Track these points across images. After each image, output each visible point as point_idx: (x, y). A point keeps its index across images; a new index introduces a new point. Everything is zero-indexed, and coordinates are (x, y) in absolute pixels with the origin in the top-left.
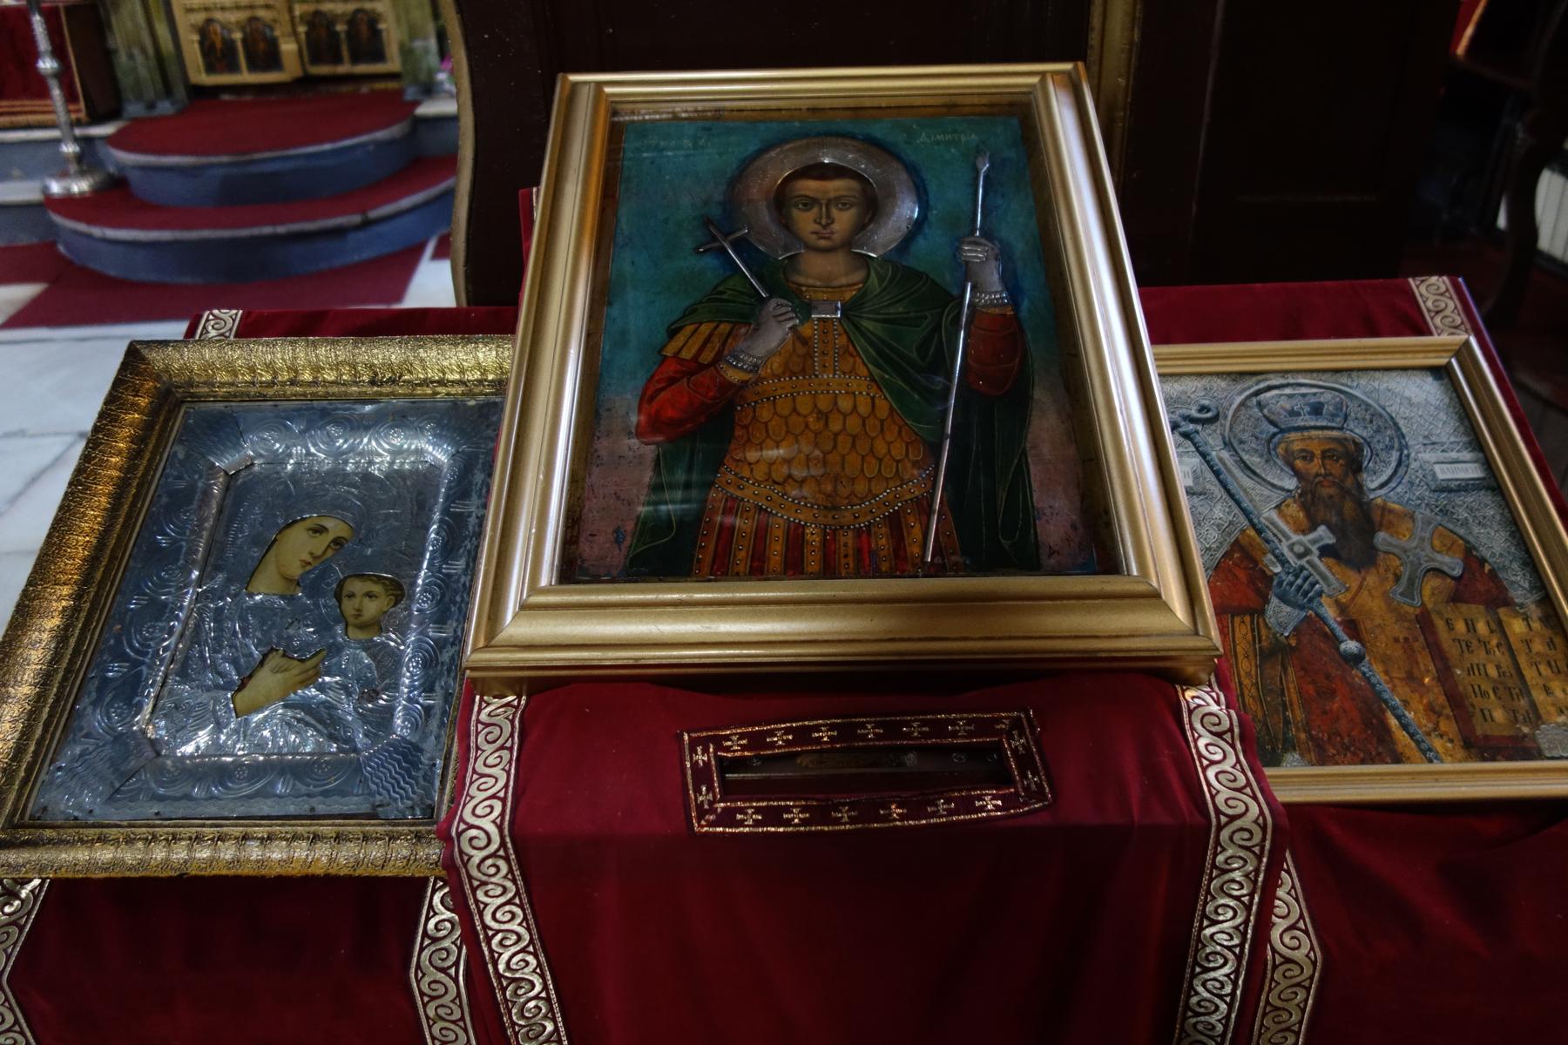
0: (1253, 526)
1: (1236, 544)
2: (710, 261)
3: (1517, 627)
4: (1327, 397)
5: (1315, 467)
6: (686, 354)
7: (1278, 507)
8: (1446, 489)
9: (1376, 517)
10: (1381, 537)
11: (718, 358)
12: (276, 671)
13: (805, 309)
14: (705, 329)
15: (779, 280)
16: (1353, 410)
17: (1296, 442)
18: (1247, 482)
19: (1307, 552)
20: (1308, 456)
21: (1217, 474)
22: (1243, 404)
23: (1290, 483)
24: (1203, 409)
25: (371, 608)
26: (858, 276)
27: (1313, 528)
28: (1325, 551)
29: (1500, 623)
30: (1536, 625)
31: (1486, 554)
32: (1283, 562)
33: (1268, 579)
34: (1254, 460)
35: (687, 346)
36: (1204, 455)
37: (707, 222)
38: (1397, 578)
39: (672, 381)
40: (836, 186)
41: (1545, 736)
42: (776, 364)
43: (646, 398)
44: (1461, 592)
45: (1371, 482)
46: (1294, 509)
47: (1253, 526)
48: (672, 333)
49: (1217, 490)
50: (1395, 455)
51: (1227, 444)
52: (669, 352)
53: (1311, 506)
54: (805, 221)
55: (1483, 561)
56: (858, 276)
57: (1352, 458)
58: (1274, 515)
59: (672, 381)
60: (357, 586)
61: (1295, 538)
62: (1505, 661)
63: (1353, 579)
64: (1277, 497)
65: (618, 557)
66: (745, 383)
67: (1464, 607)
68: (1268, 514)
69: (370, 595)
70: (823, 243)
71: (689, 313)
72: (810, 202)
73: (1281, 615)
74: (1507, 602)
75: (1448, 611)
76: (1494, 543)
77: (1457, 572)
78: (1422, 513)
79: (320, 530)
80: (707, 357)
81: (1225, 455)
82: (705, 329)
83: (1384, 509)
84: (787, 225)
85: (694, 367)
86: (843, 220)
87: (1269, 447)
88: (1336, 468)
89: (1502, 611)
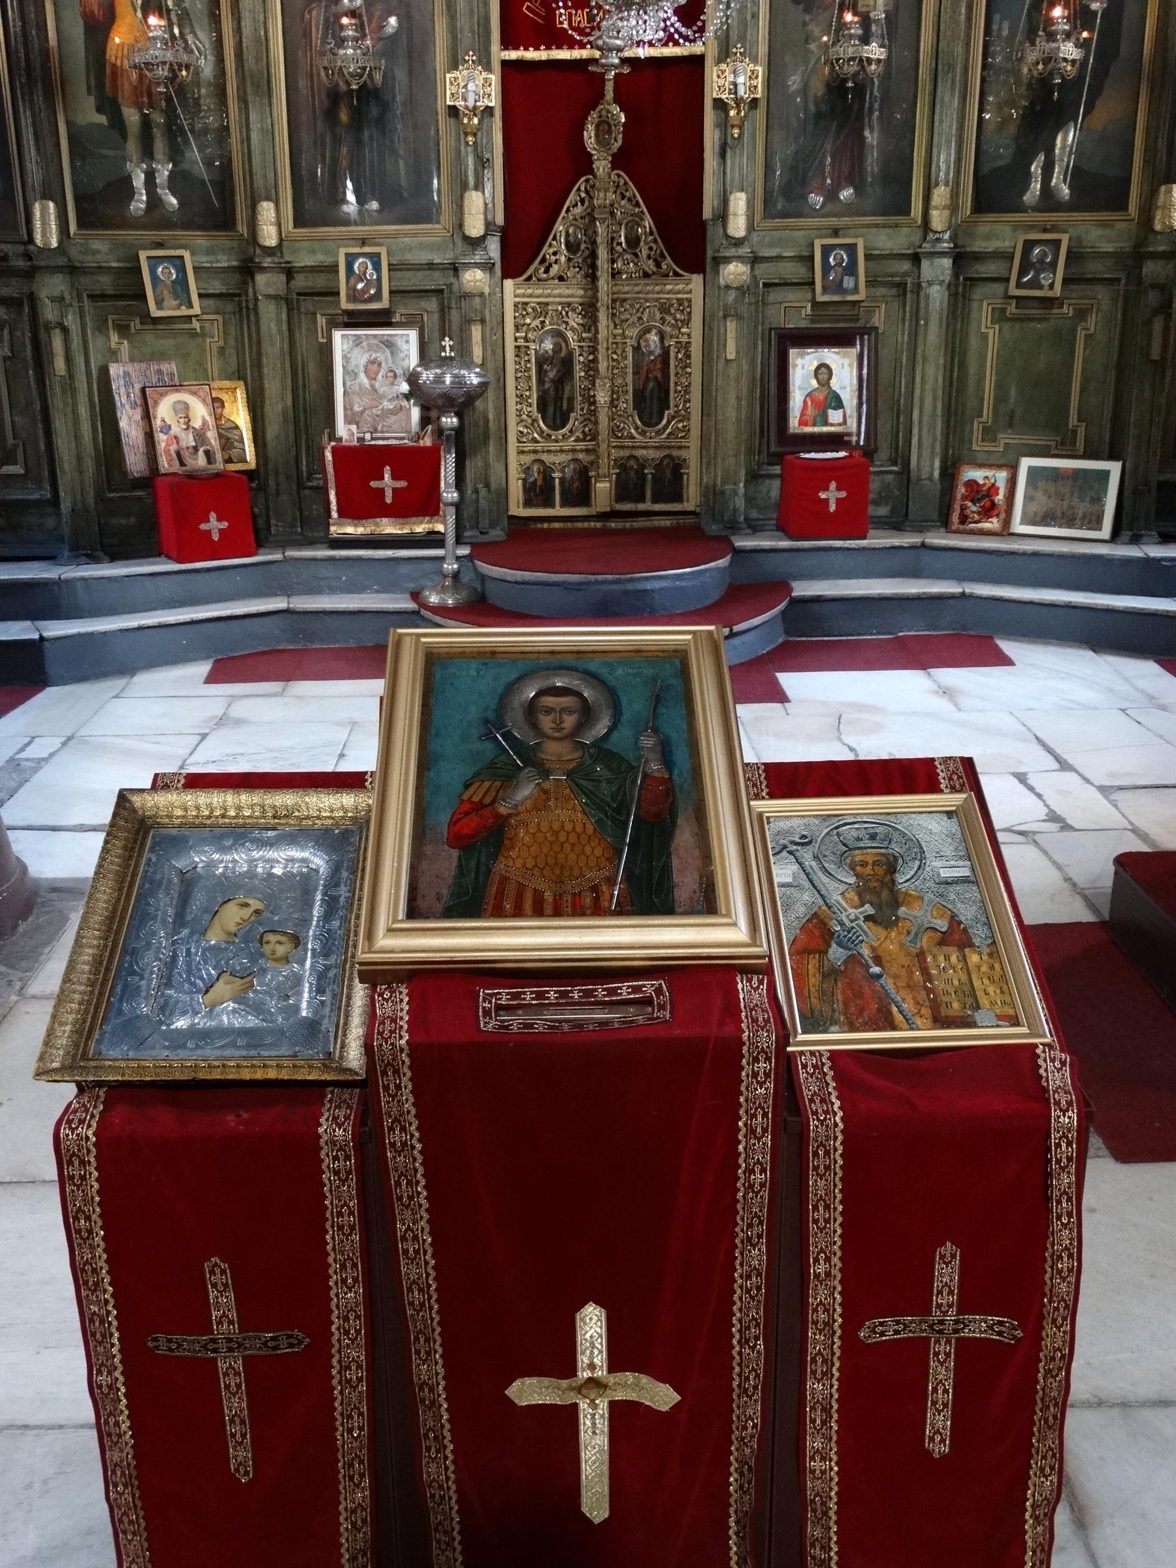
0: (827, 904)
1: (815, 915)
2: (488, 746)
3: (974, 958)
4: (880, 829)
5: (868, 870)
6: (475, 799)
7: (842, 894)
8: (947, 883)
9: (901, 899)
10: (902, 910)
11: (493, 802)
12: (227, 983)
13: (545, 773)
14: (487, 784)
15: (531, 757)
16: (896, 836)
17: (858, 856)
18: (825, 879)
19: (857, 918)
20: (864, 864)
21: (807, 875)
22: (828, 834)
23: (852, 880)
24: (804, 837)
25: (281, 950)
26: (576, 755)
27: (862, 905)
28: (868, 918)
29: (964, 957)
30: (985, 957)
31: (962, 918)
32: (842, 924)
33: (832, 934)
34: (831, 867)
35: (476, 794)
36: (800, 864)
37: (486, 722)
38: (909, 933)
39: (467, 813)
40: (566, 701)
41: (978, 1016)
42: (529, 803)
43: (453, 823)
44: (944, 940)
45: (900, 879)
46: (852, 895)
47: (827, 904)
48: (467, 786)
49: (807, 884)
50: (917, 863)
51: (816, 858)
52: (465, 797)
53: (863, 893)
54: (546, 722)
55: (960, 923)
56: (576, 755)
57: (891, 866)
58: (839, 898)
59: (467, 813)
60: (272, 938)
61: (850, 911)
62: (964, 978)
63: (882, 933)
64: (842, 888)
65: (439, 907)
66: (510, 815)
67: (945, 948)
68: (835, 897)
69: (279, 943)
70: (557, 735)
71: (477, 775)
72: (549, 711)
73: (836, 953)
74: (971, 945)
75: (935, 950)
76: (967, 913)
77: (944, 930)
78: (929, 897)
79: (247, 905)
80: (488, 800)
81: (814, 864)
82: (487, 784)
83: (906, 894)
84: (534, 725)
85: (480, 806)
86: (570, 721)
87: (841, 860)
88: (880, 871)
89: (967, 950)
